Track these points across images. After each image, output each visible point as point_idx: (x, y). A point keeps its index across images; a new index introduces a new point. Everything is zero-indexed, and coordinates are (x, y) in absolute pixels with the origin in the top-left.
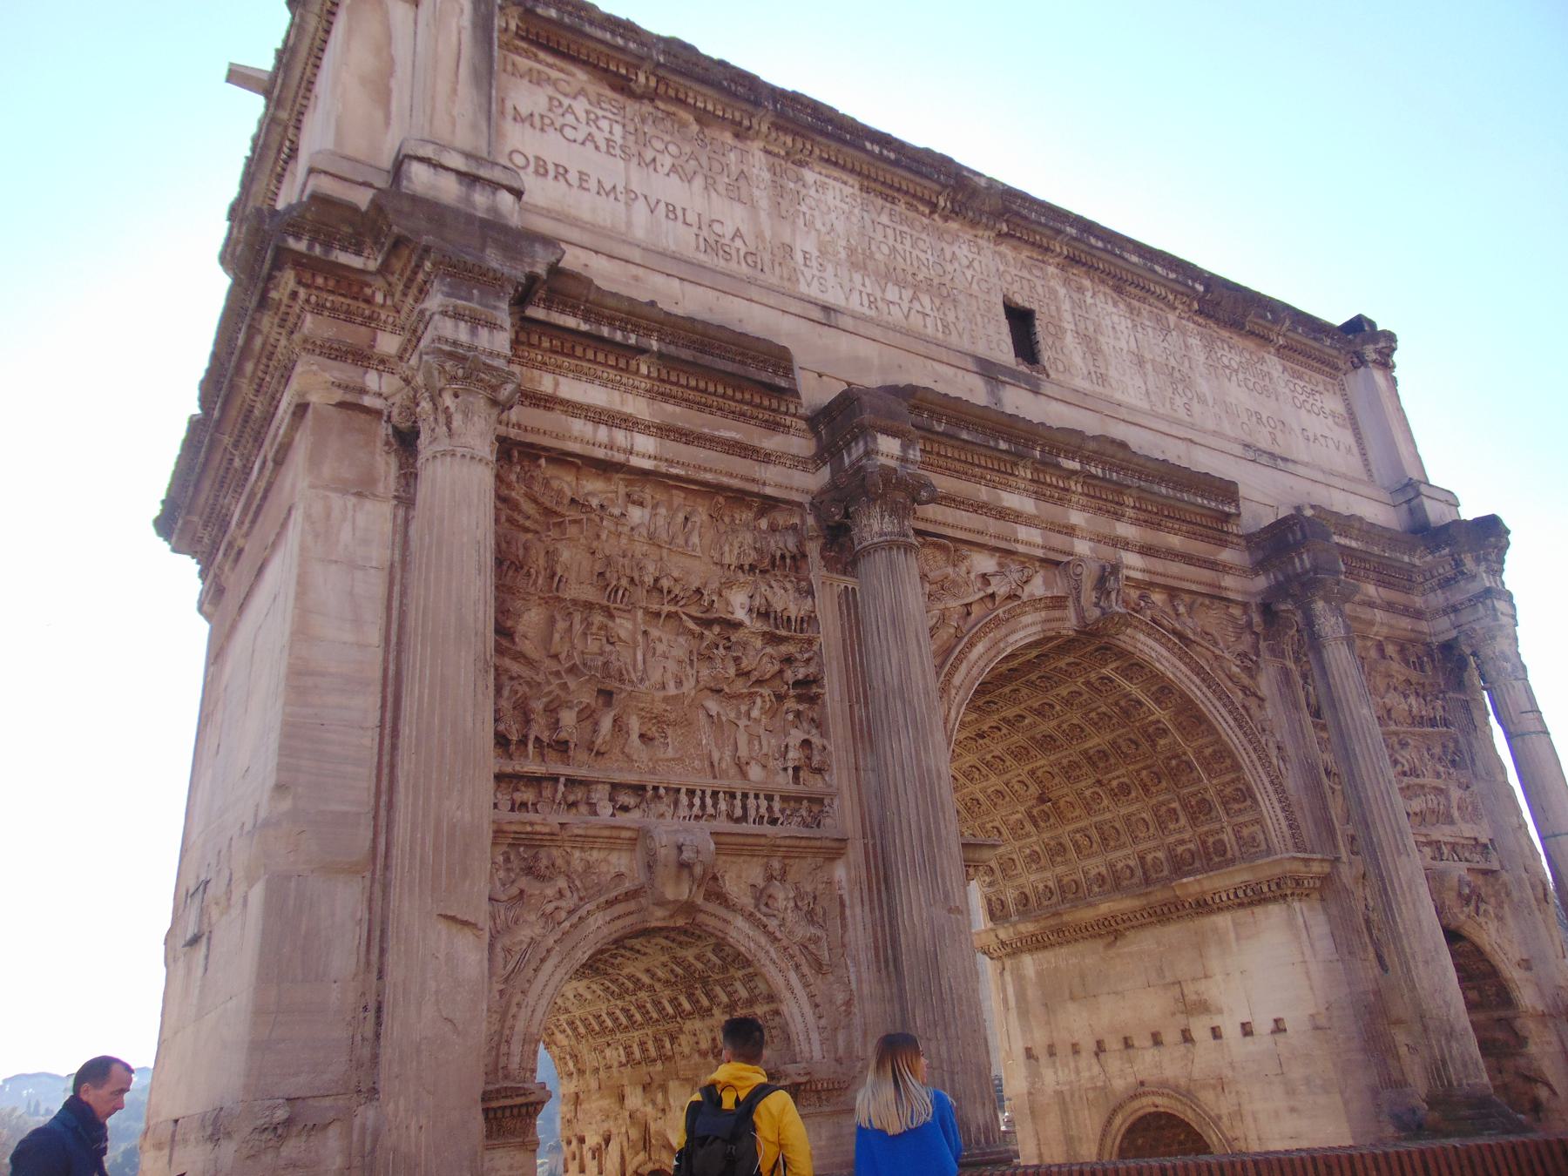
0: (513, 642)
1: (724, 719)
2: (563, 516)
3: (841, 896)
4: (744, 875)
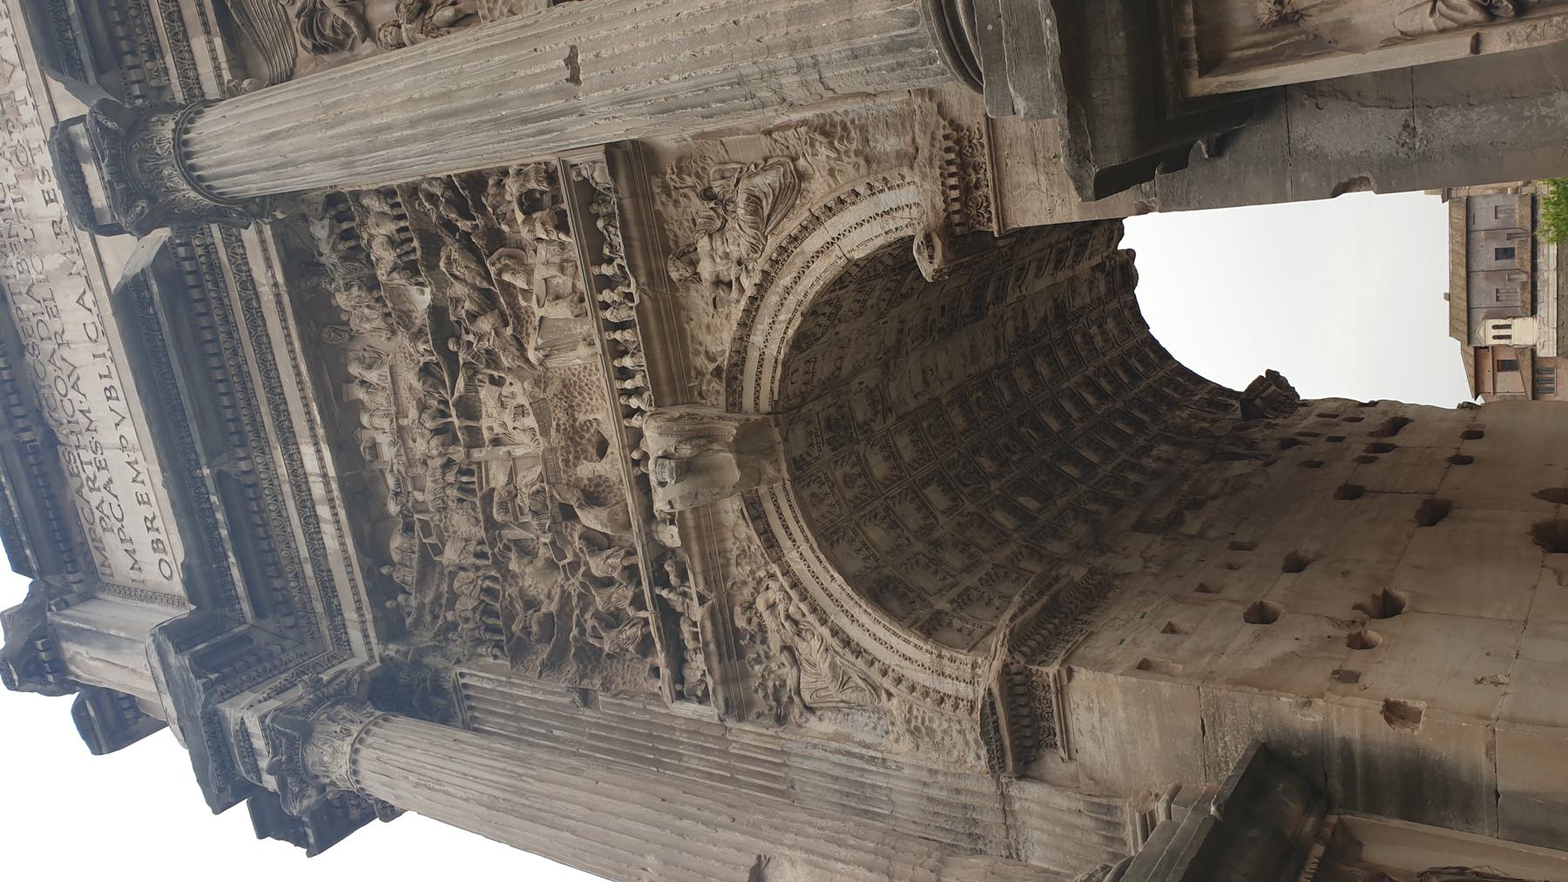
1: (540, 342)
2: (423, 545)
3: (695, 137)
4: (705, 320)
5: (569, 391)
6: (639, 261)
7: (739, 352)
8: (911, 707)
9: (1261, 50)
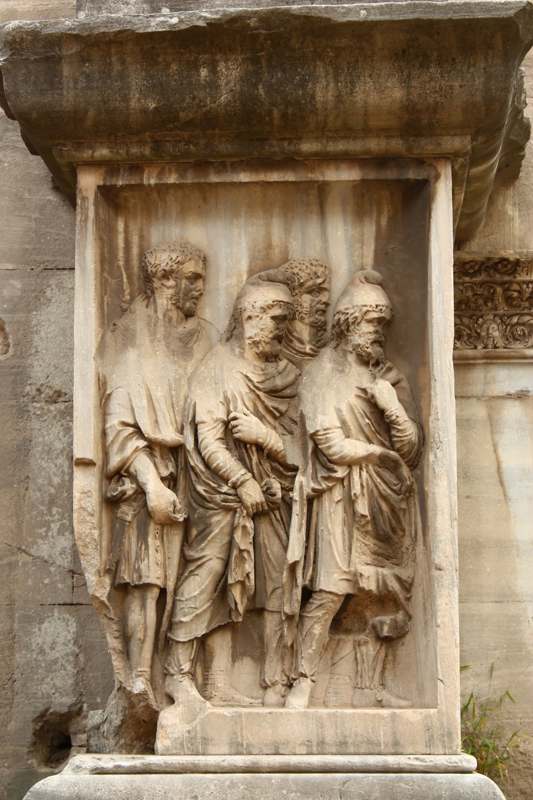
9: (121, 254)
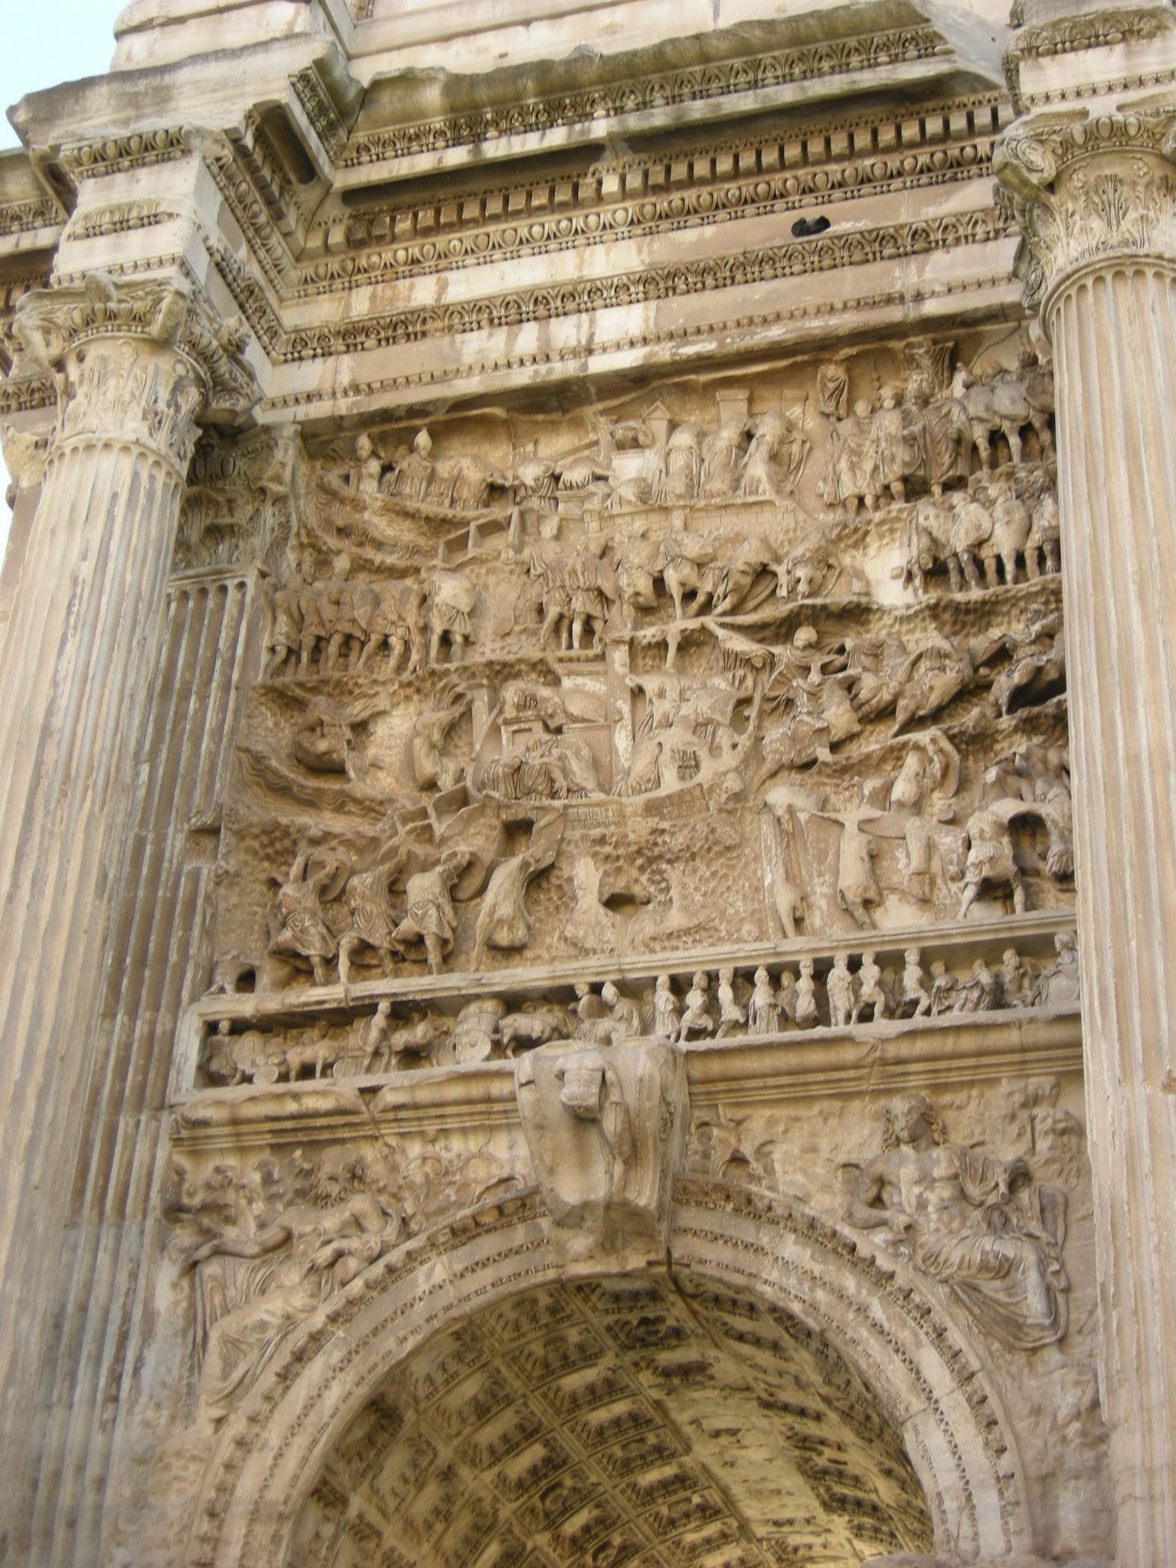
0: (349, 780)
1: (803, 817)
2: (465, 523)
4: (824, 1144)
5: (720, 854)
6: (921, 1046)
7: (770, 1208)
8: (201, 1460)
